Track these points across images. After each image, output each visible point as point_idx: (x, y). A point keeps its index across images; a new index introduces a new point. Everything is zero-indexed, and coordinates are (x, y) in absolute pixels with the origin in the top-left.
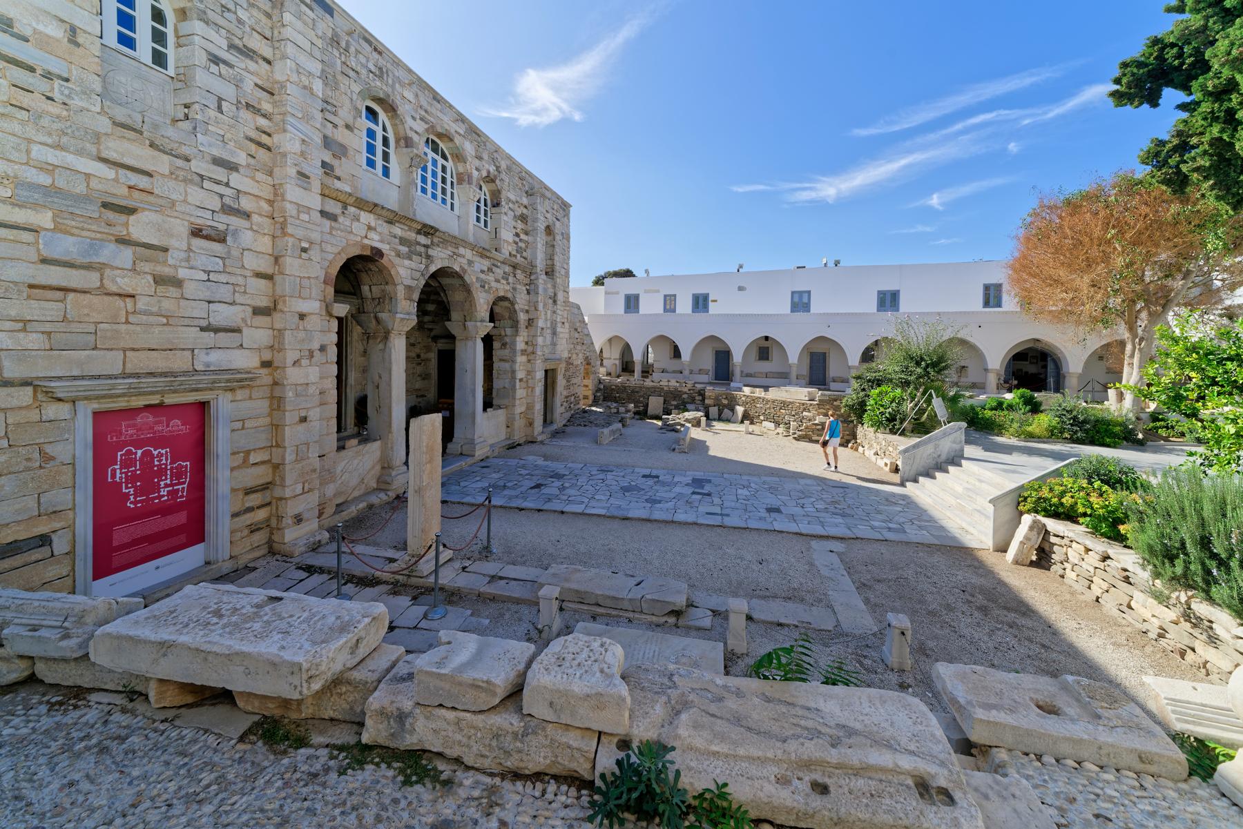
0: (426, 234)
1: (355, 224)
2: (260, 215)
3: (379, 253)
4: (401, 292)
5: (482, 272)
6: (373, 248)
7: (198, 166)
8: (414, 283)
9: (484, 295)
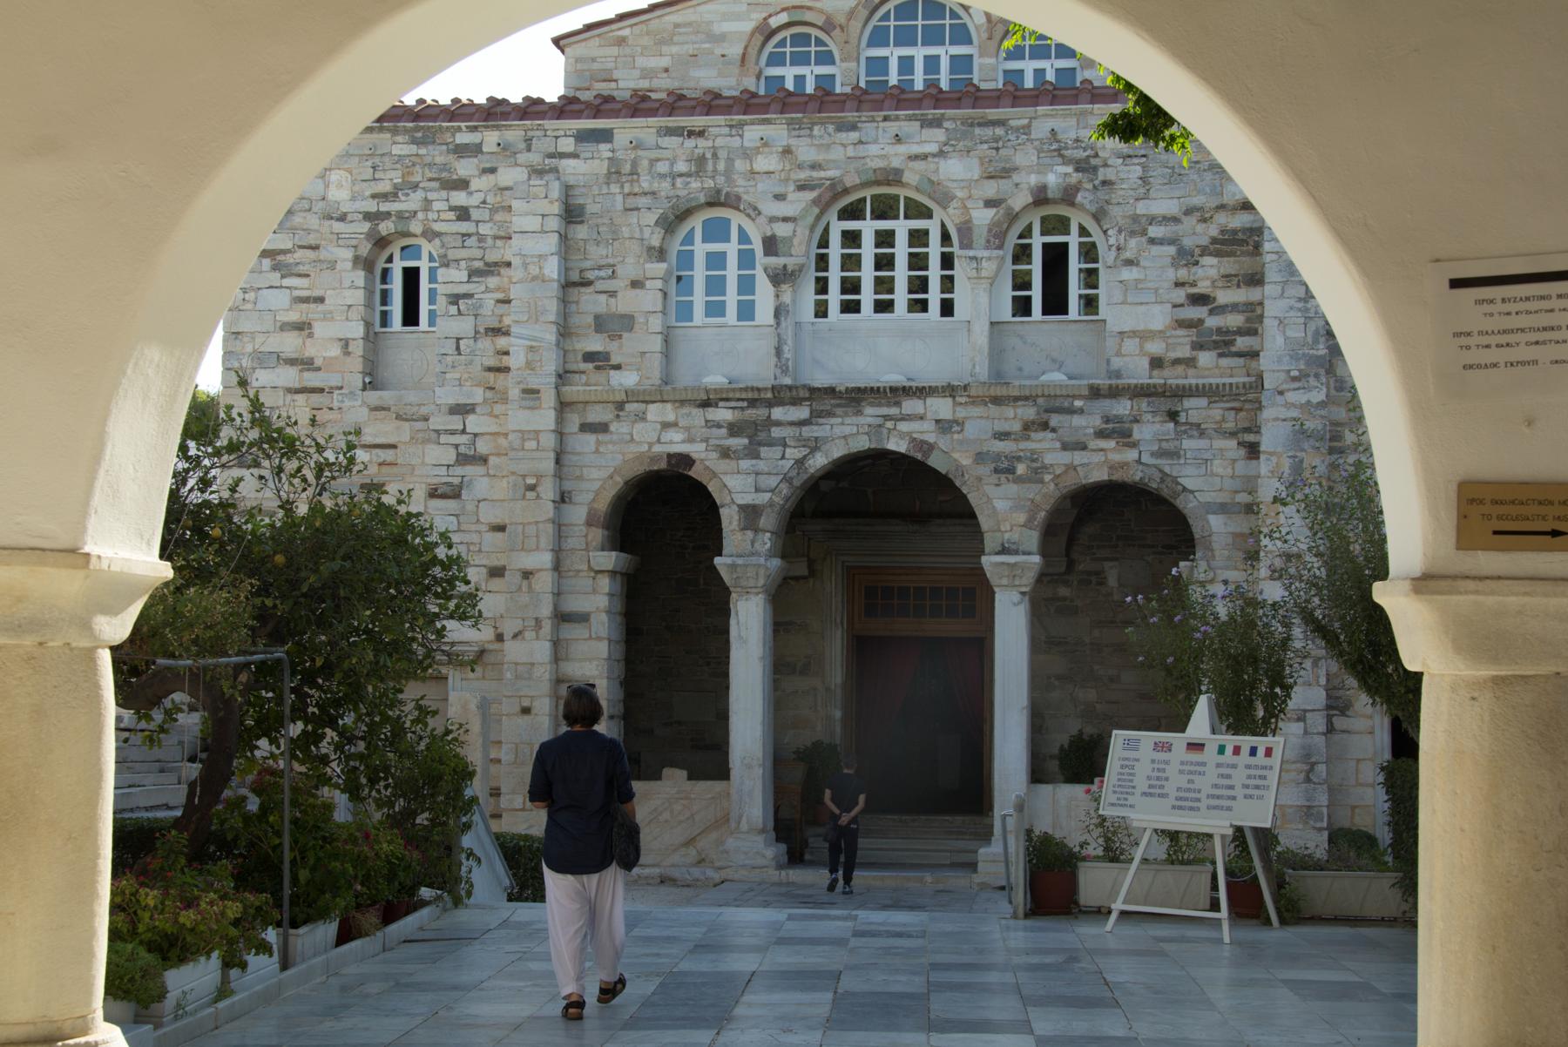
0: (795, 402)
1: (639, 426)
2: (498, 455)
3: (686, 460)
4: (729, 518)
5: (1002, 436)
6: (670, 456)
7: (437, 422)
8: (765, 497)
9: (1013, 489)
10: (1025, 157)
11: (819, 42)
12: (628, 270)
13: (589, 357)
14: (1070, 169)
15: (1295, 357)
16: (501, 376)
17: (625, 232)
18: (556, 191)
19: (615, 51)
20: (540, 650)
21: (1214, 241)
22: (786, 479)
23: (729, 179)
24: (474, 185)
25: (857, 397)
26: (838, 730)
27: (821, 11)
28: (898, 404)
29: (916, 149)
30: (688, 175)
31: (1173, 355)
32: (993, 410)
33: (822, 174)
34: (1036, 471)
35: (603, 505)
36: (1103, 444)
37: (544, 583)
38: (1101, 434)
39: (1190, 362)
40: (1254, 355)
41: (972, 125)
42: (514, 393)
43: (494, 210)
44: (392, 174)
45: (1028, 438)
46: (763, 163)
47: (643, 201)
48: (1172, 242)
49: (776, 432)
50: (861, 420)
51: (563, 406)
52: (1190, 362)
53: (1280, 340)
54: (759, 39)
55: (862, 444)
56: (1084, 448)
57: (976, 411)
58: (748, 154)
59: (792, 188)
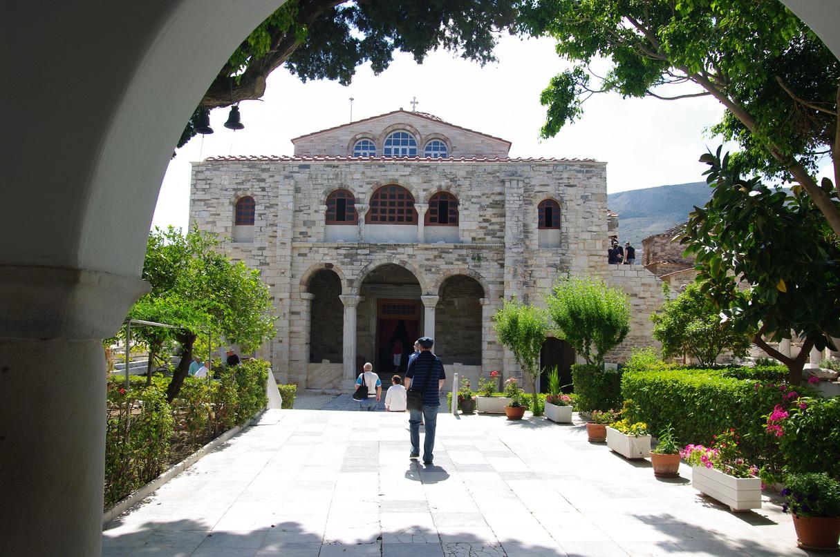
0: (365, 248)
3: (331, 265)
4: (344, 283)
5: (428, 260)
6: (326, 264)
7: (255, 252)
8: (355, 277)
9: (430, 276)
10: (435, 177)
11: (371, 143)
12: (314, 207)
13: (301, 233)
14: (448, 181)
15: (515, 238)
16: (274, 239)
17: (313, 196)
18: (292, 182)
19: (309, 144)
20: (286, 323)
21: (491, 203)
22: (362, 271)
23: (345, 180)
24: (267, 181)
25: (383, 248)
26: (374, 347)
27: (371, 134)
28: (396, 249)
29: (402, 173)
30: (333, 179)
31: (478, 237)
32: (426, 252)
33: (374, 180)
34: (438, 270)
35: (305, 278)
36: (458, 263)
37: (287, 302)
38: (457, 260)
39: (484, 239)
40: (503, 237)
41: (419, 167)
42: (278, 244)
43: (273, 188)
44: (242, 177)
45: (435, 261)
46: (356, 176)
47: (319, 187)
48: (479, 203)
49: (359, 257)
50: (383, 254)
51: (293, 248)
52: (484, 239)
53: (510, 233)
54: (353, 142)
55: (385, 261)
56: (452, 264)
57: (419, 252)
58: (351, 173)
59: (365, 183)
